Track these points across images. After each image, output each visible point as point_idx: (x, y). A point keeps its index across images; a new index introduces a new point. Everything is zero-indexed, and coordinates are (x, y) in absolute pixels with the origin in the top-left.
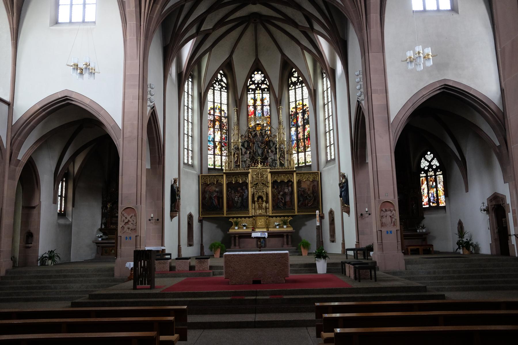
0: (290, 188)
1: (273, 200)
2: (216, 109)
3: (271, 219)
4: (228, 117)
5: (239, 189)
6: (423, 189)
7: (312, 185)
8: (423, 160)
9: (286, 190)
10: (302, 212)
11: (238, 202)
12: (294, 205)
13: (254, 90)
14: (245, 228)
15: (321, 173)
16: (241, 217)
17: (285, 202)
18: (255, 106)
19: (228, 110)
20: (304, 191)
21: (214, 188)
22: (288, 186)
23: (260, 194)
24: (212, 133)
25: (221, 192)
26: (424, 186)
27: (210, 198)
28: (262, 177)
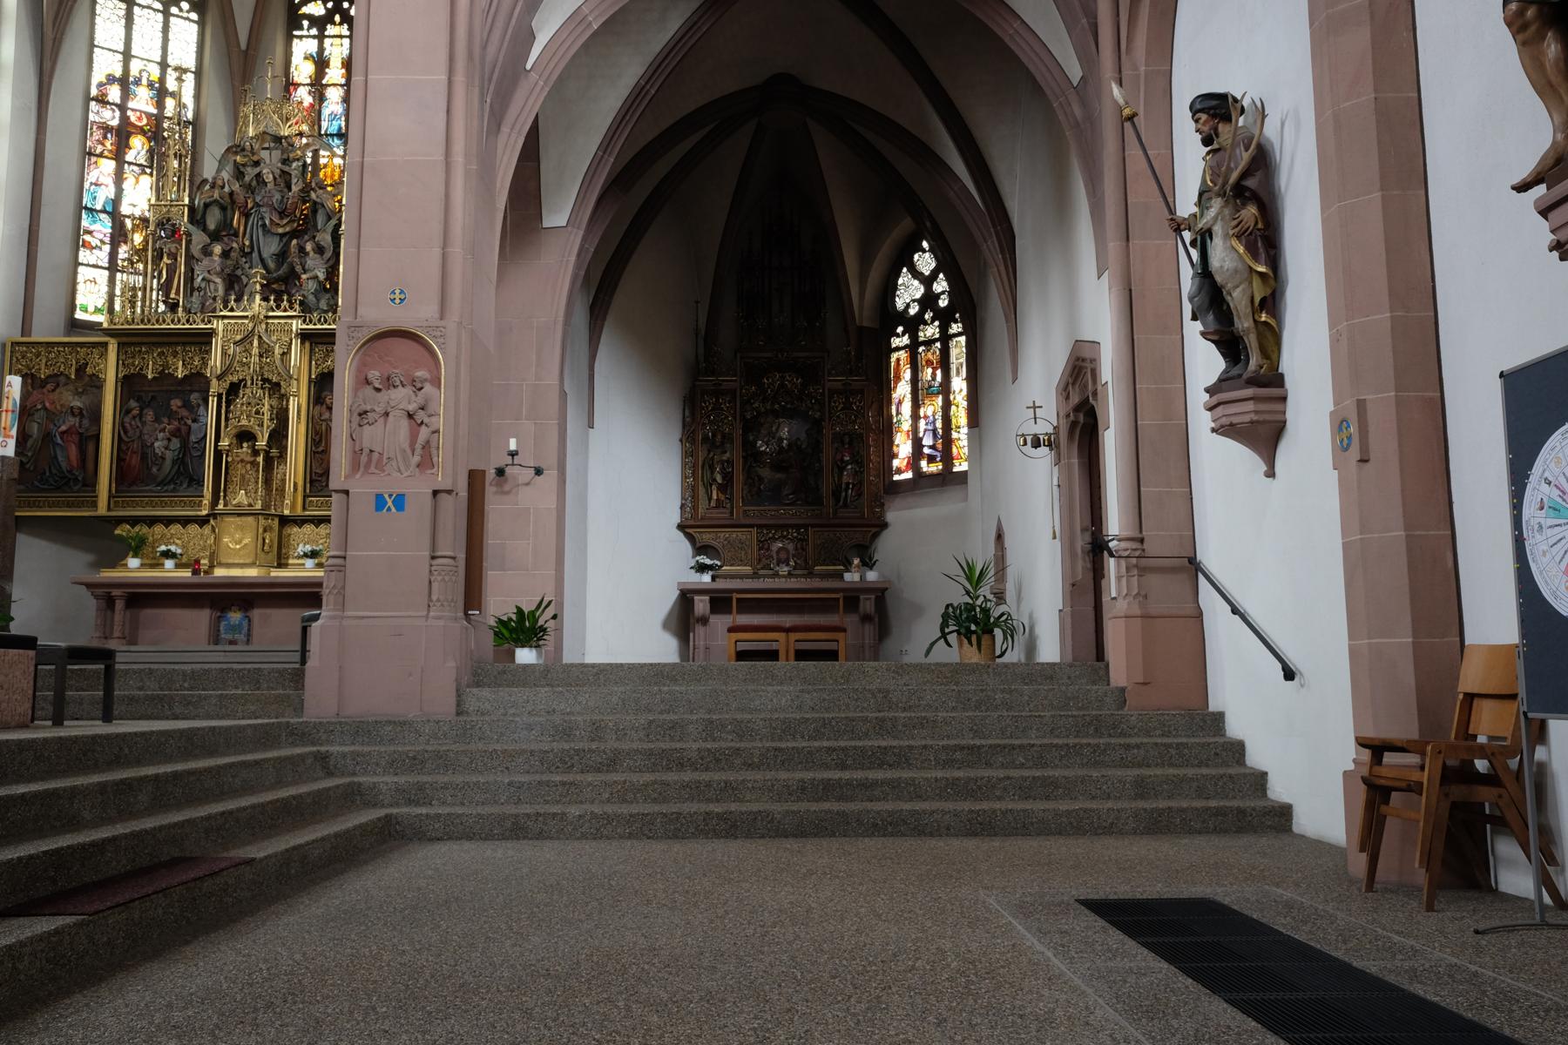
2: (138, 82)
4: (196, 124)
5: (176, 403)
6: (900, 403)
8: (905, 278)
11: (163, 458)
13: (320, 23)
14: (169, 564)
16: (152, 521)
18: (318, 87)
19: (197, 96)
23: (244, 422)
24: (109, 180)
25: (96, 417)
26: (903, 390)
27: (47, 437)
28: (266, 351)
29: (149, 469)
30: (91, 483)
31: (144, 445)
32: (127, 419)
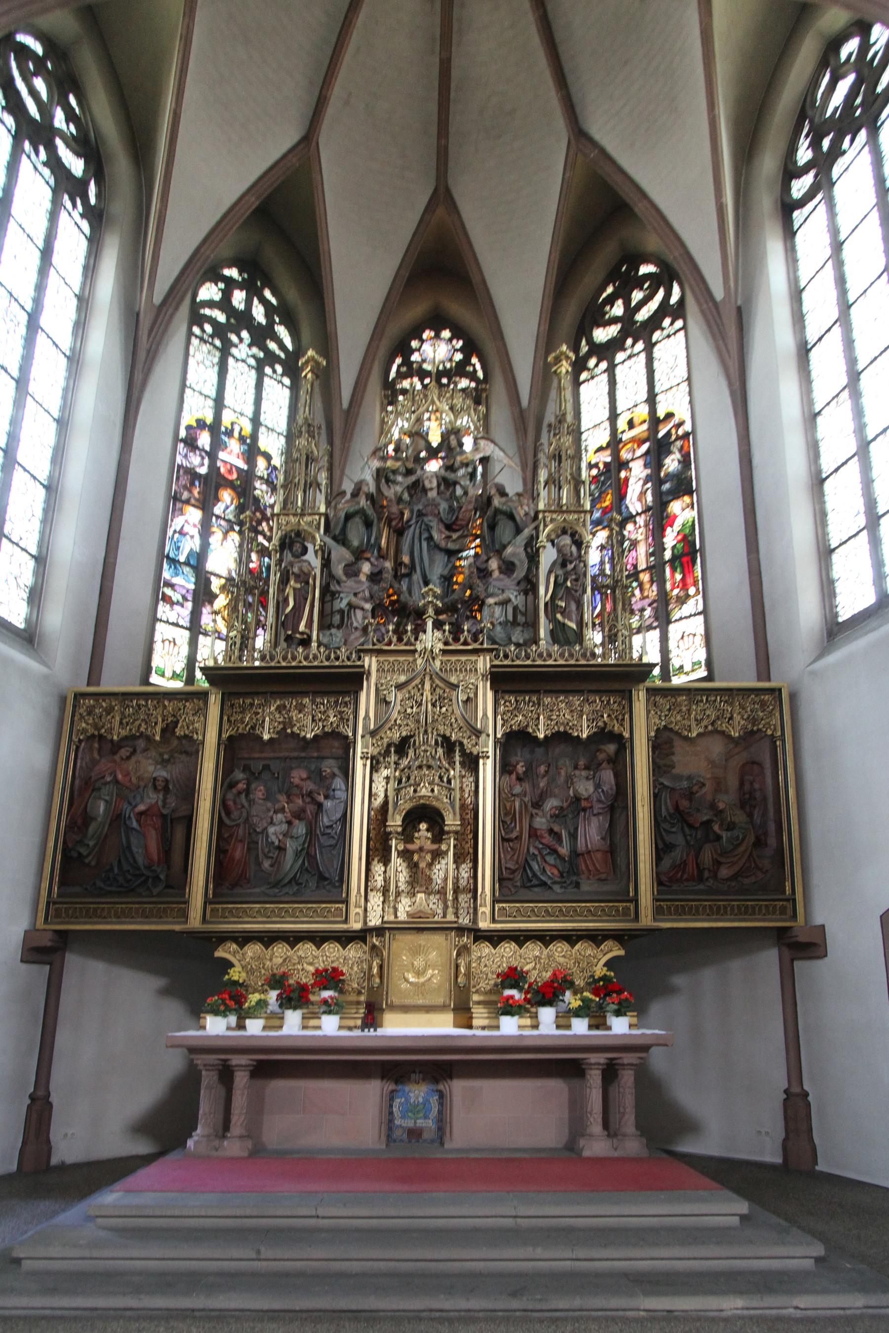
0: (608, 776)
1: (503, 839)
3: (486, 949)
9: (585, 788)
10: (681, 912)
11: (281, 849)
12: (630, 873)
17: (575, 854)
22: (593, 766)
29: (259, 864)
31: (252, 830)
32: (230, 796)
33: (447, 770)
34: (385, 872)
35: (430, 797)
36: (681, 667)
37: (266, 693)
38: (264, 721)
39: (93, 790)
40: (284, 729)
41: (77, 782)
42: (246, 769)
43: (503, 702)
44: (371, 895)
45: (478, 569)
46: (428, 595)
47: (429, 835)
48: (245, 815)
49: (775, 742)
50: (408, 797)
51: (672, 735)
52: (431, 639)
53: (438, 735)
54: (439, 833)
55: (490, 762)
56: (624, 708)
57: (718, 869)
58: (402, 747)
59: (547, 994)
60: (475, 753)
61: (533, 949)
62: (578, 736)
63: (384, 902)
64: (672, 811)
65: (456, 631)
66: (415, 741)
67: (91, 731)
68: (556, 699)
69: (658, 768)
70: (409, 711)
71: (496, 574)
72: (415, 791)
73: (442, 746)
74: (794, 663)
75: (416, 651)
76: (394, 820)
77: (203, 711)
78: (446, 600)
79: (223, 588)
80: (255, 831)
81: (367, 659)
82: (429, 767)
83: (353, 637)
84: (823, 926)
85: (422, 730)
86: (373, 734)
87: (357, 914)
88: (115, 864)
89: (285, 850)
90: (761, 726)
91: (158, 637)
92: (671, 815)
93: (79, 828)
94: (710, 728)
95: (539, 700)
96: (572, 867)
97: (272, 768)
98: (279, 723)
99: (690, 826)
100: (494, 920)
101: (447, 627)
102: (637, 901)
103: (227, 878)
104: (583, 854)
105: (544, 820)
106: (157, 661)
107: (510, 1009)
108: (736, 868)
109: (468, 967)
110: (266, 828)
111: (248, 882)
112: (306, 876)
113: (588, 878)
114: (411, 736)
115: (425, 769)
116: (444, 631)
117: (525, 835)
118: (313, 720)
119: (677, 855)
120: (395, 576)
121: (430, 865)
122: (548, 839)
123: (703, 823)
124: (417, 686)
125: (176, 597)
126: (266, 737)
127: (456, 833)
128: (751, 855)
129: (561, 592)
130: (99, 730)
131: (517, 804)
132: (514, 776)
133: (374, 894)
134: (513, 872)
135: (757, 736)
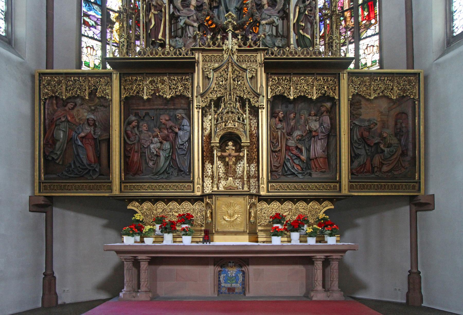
0: (326, 119)
1: (272, 151)
3: (265, 205)
7: (393, 113)
9: (314, 125)
11: (158, 156)
15: (426, 78)
20: (369, 129)
21: (84, 114)
22: (319, 114)
29: (147, 163)
30: (106, 172)
32: (129, 129)
33: (242, 115)
34: (212, 168)
35: (233, 128)
36: (366, 64)
37: (143, 74)
38: (143, 89)
39: (56, 125)
40: (155, 93)
41: (47, 121)
42: (136, 115)
43: (271, 80)
44: (206, 179)
45: (256, 4)
46: (229, 18)
47: (234, 148)
48: (137, 139)
49: (415, 102)
50: (221, 128)
51: (361, 98)
52: (231, 43)
53: (237, 96)
54: (239, 147)
55: (264, 111)
56: (335, 83)
57: (382, 166)
58: (218, 102)
59: (296, 226)
60: (257, 106)
61: (288, 205)
62: (311, 98)
63: (212, 183)
64: (359, 137)
65: (245, 39)
66: (224, 99)
67: (51, 94)
68: (300, 77)
69: (353, 115)
70: (221, 83)
71: (266, 7)
72: (225, 125)
73: (239, 102)
74: (426, 61)
75: (223, 50)
76: (215, 140)
77: (109, 83)
78: (239, 22)
79: (117, 18)
80: (144, 147)
81: (197, 54)
82: (232, 113)
83: (188, 42)
84: (433, 195)
85: (228, 93)
86: (202, 95)
87: (198, 187)
88: (72, 163)
89: (160, 156)
90: (408, 93)
91: (83, 45)
92: (358, 140)
93: (50, 145)
94: (381, 94)
95: (290, 78)
96: (307, 166)
97: (150, 114)
98: (152, 90)
99: (369, 145)
100: (268, 191)
101: (240, 37)
102: (340, 182)
103: (130, 170)
104: (313, 159)
105: (293, 142)
106: (84, 58)
107: (277, 233)
108: (391, 167)
109: (256, 214)
110: (149, 146)
111: (142, 173)
112: (172, 170)
113: (316, 171)
114: (223, 97)
115: (230, 114)
116: (238, 39)
117: (284, 149)
118: (170, 89)
119: (361, 160)
120: (211, 8)
121: (235, 164)
122: (295, 152)
123: (375, 144)
124: (224, 69)
125: (91, 23)
126: (145, 97)
127: (248, 147)
128: (399, 160)
129: (302, 18)
130: (55, 93)
131: (279, 133)
132: (277, 119)
133: (207, 178)
134: (278, 168)
135: (405, 99)
